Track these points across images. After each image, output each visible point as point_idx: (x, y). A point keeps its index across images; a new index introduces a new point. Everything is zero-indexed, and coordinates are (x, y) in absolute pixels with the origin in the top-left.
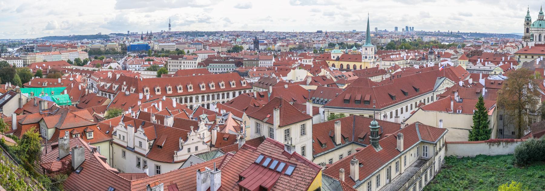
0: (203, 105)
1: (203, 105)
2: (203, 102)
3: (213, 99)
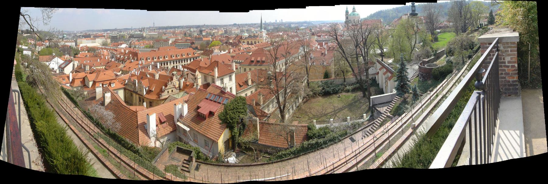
0: (174, 66)
1: (174, 66)
2: (174, 65)
3: (179, 63)
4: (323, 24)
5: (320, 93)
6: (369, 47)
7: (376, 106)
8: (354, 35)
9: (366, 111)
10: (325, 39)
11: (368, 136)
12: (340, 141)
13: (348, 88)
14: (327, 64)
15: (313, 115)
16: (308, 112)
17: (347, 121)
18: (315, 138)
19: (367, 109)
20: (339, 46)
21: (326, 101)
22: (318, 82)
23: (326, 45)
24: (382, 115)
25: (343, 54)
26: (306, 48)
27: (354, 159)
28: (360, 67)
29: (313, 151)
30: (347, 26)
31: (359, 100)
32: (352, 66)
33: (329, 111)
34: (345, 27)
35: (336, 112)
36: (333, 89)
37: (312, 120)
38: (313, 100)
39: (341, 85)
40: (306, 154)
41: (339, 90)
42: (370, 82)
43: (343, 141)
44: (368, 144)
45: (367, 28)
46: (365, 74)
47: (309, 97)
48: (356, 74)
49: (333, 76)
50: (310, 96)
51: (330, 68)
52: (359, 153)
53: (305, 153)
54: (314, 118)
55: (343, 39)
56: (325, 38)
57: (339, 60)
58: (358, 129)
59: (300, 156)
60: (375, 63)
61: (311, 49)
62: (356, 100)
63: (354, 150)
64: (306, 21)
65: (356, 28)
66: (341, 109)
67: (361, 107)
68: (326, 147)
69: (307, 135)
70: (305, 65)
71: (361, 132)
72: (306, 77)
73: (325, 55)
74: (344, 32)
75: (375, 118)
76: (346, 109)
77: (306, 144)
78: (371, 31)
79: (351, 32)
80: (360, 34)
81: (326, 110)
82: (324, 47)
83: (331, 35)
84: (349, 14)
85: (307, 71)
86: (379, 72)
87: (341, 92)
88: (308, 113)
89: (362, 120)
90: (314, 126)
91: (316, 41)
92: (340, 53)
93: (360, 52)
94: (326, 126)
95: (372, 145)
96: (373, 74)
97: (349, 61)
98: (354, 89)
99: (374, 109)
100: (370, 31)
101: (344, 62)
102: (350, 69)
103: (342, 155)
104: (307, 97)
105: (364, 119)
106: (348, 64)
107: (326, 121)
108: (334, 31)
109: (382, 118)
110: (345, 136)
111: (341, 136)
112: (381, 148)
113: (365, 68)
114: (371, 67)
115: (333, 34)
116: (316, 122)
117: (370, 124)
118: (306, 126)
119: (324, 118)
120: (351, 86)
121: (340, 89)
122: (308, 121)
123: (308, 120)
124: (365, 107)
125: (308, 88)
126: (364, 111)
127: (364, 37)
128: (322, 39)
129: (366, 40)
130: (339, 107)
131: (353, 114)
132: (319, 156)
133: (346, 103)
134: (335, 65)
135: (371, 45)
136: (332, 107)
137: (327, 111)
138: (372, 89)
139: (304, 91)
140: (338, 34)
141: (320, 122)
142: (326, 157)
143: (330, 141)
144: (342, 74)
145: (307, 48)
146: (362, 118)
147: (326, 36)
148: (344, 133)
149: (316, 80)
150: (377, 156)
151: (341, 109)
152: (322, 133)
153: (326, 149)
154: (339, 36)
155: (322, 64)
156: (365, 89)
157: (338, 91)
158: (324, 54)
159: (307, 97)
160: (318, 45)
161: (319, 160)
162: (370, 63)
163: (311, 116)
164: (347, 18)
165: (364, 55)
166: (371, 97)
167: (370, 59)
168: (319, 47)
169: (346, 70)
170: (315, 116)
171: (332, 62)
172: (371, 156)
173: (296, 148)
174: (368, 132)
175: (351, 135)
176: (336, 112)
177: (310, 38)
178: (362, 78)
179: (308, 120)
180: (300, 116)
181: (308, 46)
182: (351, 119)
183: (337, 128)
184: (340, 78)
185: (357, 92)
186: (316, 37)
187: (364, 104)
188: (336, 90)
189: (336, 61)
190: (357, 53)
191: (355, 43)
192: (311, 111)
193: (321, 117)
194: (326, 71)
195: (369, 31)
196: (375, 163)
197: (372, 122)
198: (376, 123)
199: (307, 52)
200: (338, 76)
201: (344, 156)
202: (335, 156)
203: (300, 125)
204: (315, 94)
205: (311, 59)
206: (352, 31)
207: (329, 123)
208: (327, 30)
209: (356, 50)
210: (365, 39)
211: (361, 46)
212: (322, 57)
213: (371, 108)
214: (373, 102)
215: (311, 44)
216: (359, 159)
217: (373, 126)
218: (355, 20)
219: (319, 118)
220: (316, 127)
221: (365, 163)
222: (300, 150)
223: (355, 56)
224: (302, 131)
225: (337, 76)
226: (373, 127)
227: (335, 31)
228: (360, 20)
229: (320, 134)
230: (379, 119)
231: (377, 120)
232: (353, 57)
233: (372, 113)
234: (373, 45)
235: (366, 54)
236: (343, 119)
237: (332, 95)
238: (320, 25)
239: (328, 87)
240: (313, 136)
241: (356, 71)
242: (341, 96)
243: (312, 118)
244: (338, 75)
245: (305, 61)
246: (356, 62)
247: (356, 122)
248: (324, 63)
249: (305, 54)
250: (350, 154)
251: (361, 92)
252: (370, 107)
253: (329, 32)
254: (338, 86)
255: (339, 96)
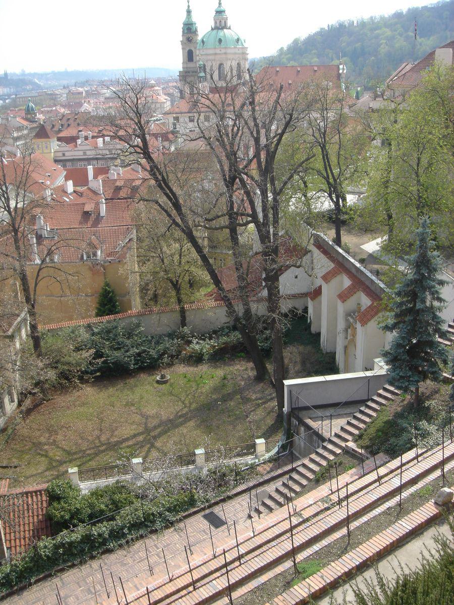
4: (82, 85)
5: (86, 372)
6: (285, 183)
7: (304, 412)
8: (219, 131)
9: (264, 428)
10: (93, 152)
11: (271, 510)
12: (169, 524)
13: (197, 347)
14: (109, 255)
15: (64, 450)
16: (45, 444)
17: (193, 462)
18: (78, 525)
19: (270, 421)
20: (156, 180)
21: (113, 399)
22: (73, 332)
23: (100, 178)
24: (325, 444)
25: (174, 213)
26: (12, 195)
27: (222, 575)
28: (245, 266)
29: (76, 562)
30: (192, 94)
31: (239, 391)
32: (211, 261)
33: (126, 431)
34: (182, 97)
35: (152, 434)
36: (139, 354)
37: (62, 469)
38: (61, 400)
39: (171, 336)
40: (50, 576)
41: (161, 356)
42: (283, 326)
43: (182, 525)
44: (269, 535)
45: (277, 102)
46: (265, 293)
47: (43, 391)
48: (230, 296)
49: (137, 305)
50: (47, 386)
51: (121, 271)
52: (239, 558)
53: (47, 573)
54: (70, 461)
55: (173, 149)
56: (96, 148)
57: (157, 239)
58: (235, 486)
59: (30, 584)
60: (307, 252)
61: (36, 197)
62: (229, 389)
63: (219, 550)
64: (6, 74)
65: (229, 100)
66: (170, 425)
67: (247, 417)
68: (121, 546)
69: (49, 518)
70: (17, 264)
71: (246, 497)
72: (23, 315)
73: (98, 219)
74: (177, 119)
75: (297, 455)
76: (192, 424)
77: (45, 547)
78: (295, 116)
79: (207, 119)
80: (246, 130)
81: (113, 432)
82: (91, 185)
83: (121, 133)
84: (200, 38)
85: (26, 289)
86: (320, 287)
87: (170, 365)
88: (46, 447)
89: (250, 459)
90: (70, 487)
91: (56, 161)
92: (163, 209)
93: (247, 204)
94: (118, 482)
95: (282, 538)
96: (294, 297)
97: (200, 241)
98: (221, 349)
99: (295, 422)
100: (291, 115)
101: (177, 245)
102: (207, 277)
103: (179, 567)
104: (36, 390)
105: (256, 457)
106: (194, 254)
107: (117, 466)
108: (132, 115)
109: (326, 454)
110: (186, 510)
111: (173, 509)
112: (316, 547)
113: (265, 270)
114: (288, 267)
115: (130, 131)
116: (80, 472)
117: (280, 471)
118: (40, 491)
119: (108, 458)
120: (210, 339)
121: (163, 354)
122: (47, 473)
123: (47, 469)
124: (262, 415)
125: (38, 356)
126: (258, 427)
127: (263, 141)
128: (81, 153)
129: (271, 156)
130: (164, 418)
131: (218, 440)
132: (99, 576)
133: (191, 404)
134: (143, 260)
135: (292, 176)
136: (137, 418)
137: (116, 433)
138: (291, 354)
139: (24, 368)
140: (153, 127)
141: (93, 470)
142: (124, 576)
143: (135, 526)
144: (174, 293)
145: (17, 196)
146: (252, 454)
147: (100, 140)
148: (185, 502)
149: (65, 324)
150: (300, 570)
151: (170, 425)
152: (103, 507)
153: (120, 553)
154: (156, 136)
155: (88, 257)
156: (263, 350)
157: (157, 360)
158: (93, 217)
159: (36, 390)
160: (67, 178)
161: (98, 587)
162: (288, 250)
163: (58, 455)
164: (190, 56)
165: (260, 216)
166: (287, 382)
167: (287, 233)
168: (70, 187)
169: (187, 278)
170: (75, 453)
171: (129, 249)
172: (279, 569)
173: (12, 566)
174: (271, 497)
175: (210, 507)
176: (152, 434)
177: (28, 150)
178: (253, 311)
179: (47, 469)
180: (15, 462)
181: (23, 183)
182: (208, 457)
183: (157, 486)
184: (163, 312)
185: (233, 360)
186: (54, 146)
187: (258, 405)
188: (151, 358)
189: (147, 242)
190: (232, 208)
191: (226, 168)
192: (54, 441)
193: (96, 454)
194: (107, 285)
195: (288, 117)
196: (291, 589)
197: (289, 467)
198: (301, 469)
199: (19, 212)
200: (156, 301)
201: (185, 568)
202: (156, 570)
203: (19, 490)
204: (64, 375)
205: (40, 238)
206: (212, 116)
207: (126, 473)
208: (101, 113)
209: (231, 197)
210: (268, 151)
211: (252, 178)
212: (87, 229)
213: (285, 417)
214: (294, 400)
215: (35, 176)
216: (236, 575)
217: (291, 478)
218: (227, 68)
219: (90, 460)
220: (79, 490)
221: (257, 588)
222: (26, 569)
223: (224, 221)
224: (28, 510)
225: (152, 303)
226: (291, 483)
227: (139, 114)
228: (247, 67)
229: (97, 509)
230: (313, 456)
231: (306, 461)
232: (214, 224)
233: (289, 435)
234: (302, 178)
235: (271, 216)
236: (180, 457)
237: (133, 377)
238: (73, 89)
239: (119, 349)
240: (72, 518)
241: (230, 283)
242: (168, 377)
243: (61, 463)
244: (155, 298)
245: (12, 248)
246: (230, 244)
247: (229, 466)
248: (95, 255)
249: (13, 219)
250: (205, 563)
251: (248, 361)
252: (280, 415)
253: (111, 121)
254: (158, 343)
255: (163, 377)
